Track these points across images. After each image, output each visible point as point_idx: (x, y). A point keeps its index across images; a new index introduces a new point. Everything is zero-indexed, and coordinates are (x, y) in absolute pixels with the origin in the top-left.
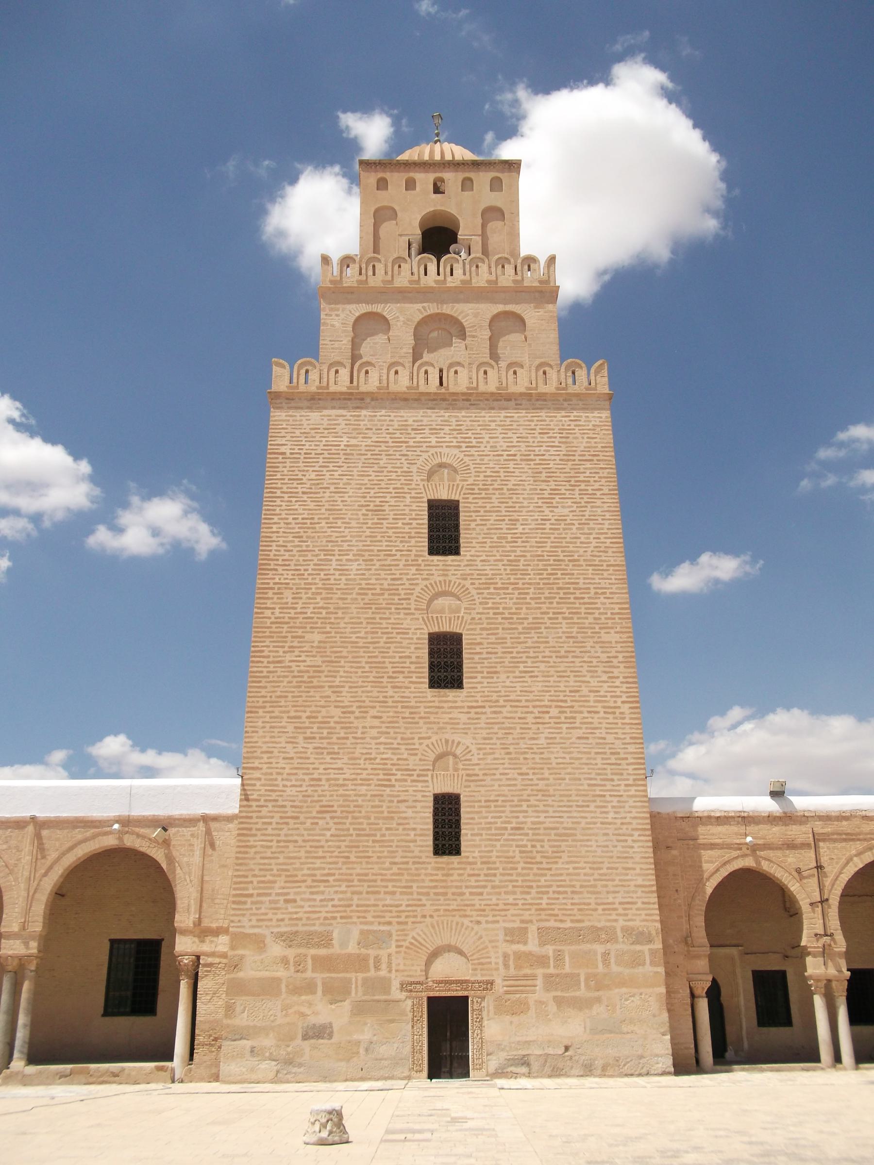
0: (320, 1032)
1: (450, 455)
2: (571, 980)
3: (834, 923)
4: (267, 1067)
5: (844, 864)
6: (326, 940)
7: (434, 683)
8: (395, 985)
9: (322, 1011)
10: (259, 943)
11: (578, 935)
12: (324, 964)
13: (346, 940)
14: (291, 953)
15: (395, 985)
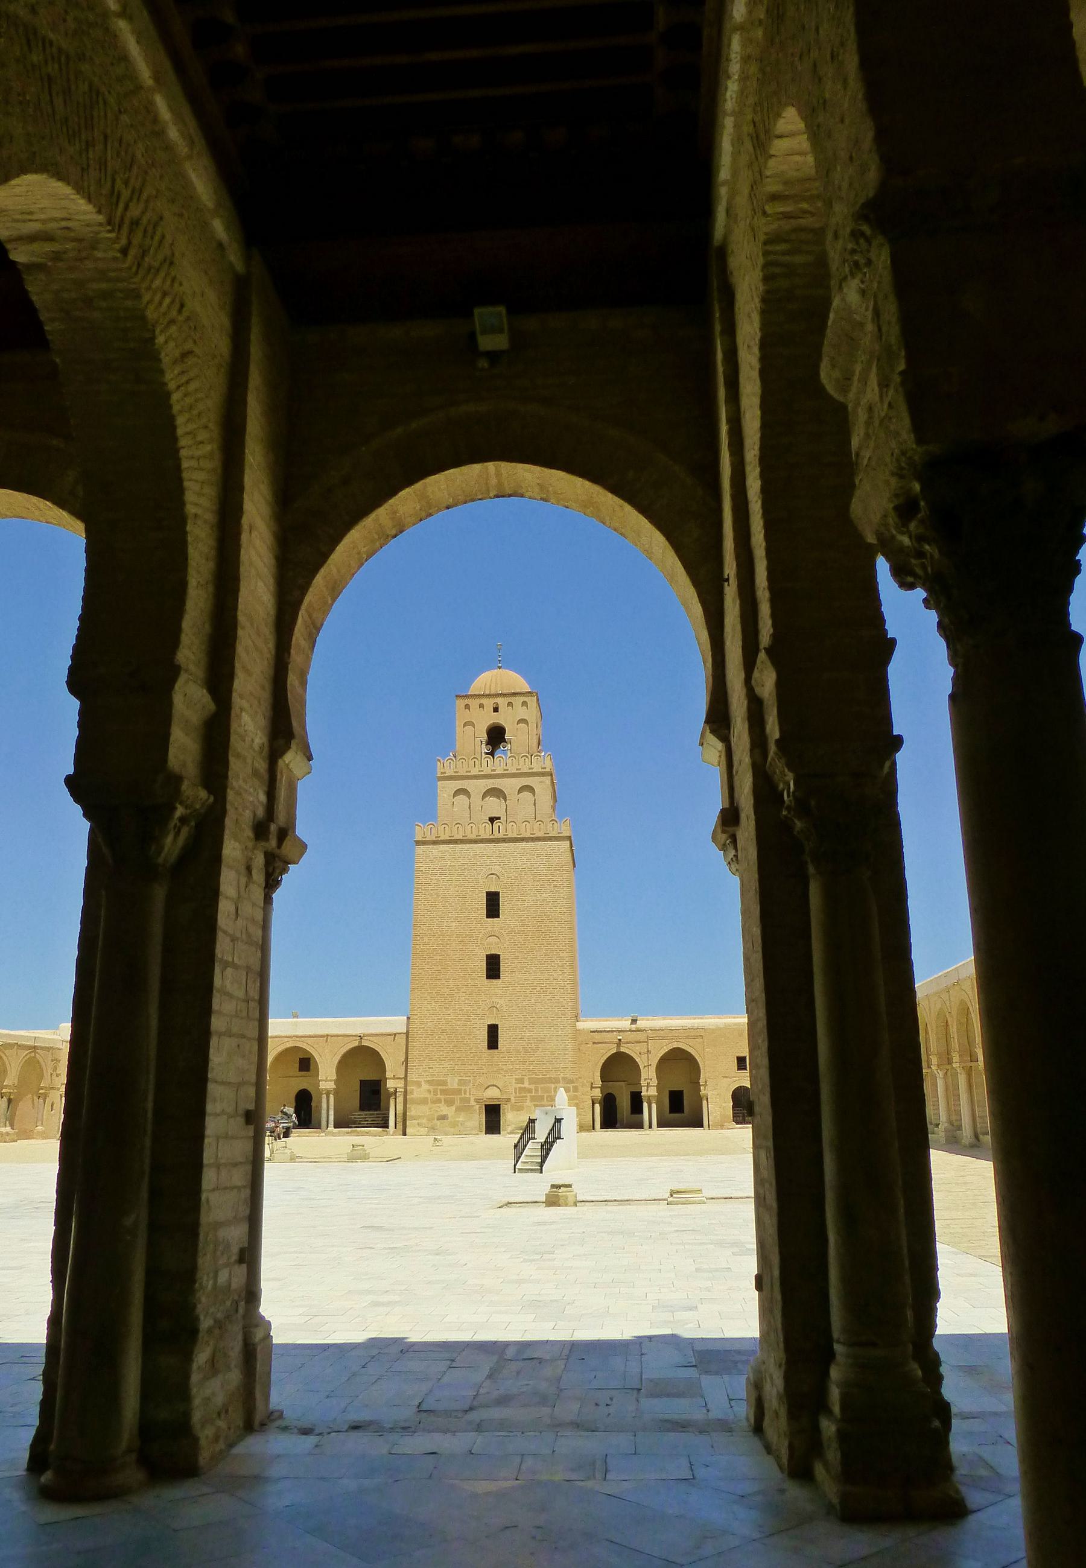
0: (443, 1118)
1: (496, 869)
2: (542, 1098)
3: (653, 1074)
4: (424, 1130)
5: (660, 1050)
6: (444, 1083)
7: (489, 977)
8: (472, 1100)
9: (444, 1110)
10: (419, 1084)
11: (543, 1081)
12: (443, 1092)
13: (453, 1083)
14: (431, 1088)
15: (472, 1100)
